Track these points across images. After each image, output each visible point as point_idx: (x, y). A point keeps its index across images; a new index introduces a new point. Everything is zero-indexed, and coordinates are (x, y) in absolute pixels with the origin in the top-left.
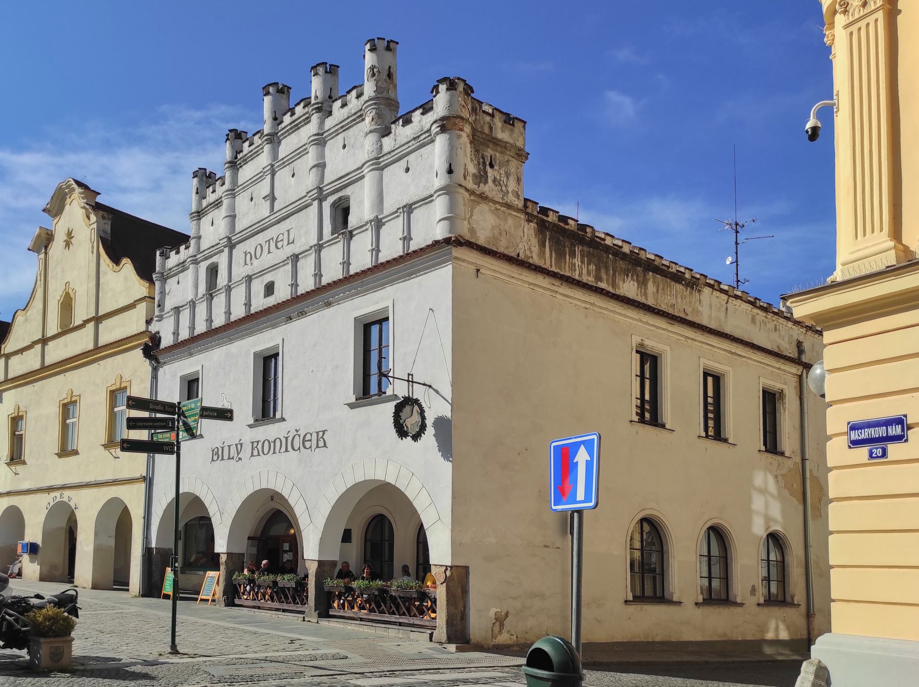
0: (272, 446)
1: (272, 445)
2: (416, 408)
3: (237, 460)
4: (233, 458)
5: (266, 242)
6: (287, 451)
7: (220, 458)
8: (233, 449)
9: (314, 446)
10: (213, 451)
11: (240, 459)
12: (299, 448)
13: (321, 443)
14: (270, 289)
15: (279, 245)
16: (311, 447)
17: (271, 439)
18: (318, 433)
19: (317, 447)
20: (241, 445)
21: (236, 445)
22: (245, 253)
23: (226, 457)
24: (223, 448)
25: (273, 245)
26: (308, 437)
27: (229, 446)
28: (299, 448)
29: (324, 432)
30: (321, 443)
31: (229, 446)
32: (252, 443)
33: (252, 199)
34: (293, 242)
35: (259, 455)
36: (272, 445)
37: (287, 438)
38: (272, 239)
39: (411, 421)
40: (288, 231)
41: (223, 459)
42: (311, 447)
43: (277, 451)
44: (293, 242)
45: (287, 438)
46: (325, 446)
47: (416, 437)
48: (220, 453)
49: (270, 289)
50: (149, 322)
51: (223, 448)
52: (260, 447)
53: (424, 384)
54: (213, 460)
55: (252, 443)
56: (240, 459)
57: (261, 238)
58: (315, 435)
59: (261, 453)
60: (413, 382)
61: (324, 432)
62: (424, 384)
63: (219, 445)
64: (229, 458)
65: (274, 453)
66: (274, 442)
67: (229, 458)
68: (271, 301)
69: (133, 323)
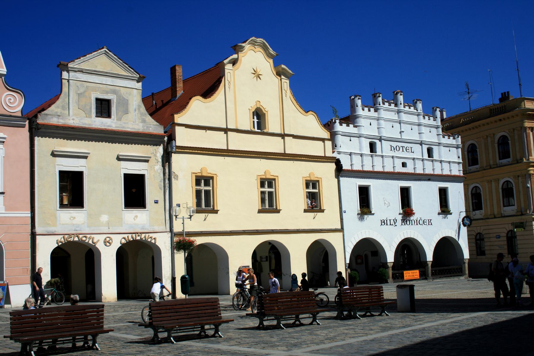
3: (395, 226)
4: (392, 225)
5: (401, 147)
6: (417, 224)
8: (392, 221)
9: (428, 224)
10: (381, 221)
11: (396, 225)
12: (422, 224)
13: (430, 224)
16: (426, 224)
18: (428, 220)
19: (429, 224)
20: (396, 220)
21: (394, 220)
22: (391, 146)
24: (387, 220)
26: (425, 221)
28: (422, 224)
30: (430, 224)
31: (390, 220)
34: (413, 152)
35: (405, 225)
37: (417, 220)
38: (404, 147)
42: (426, 224)
43: (413, 224)
45: (417, 220)
46: (431, 224)
48: (385, 222)
51: (387, 220)
54: (382, 225)
56: (396, 225)
58: (427, 221)
61: (431, 220)
63: (385, 219)
64: (390, 225)
65: (412, 225)
67: (390, 225)
68: (404, 170)
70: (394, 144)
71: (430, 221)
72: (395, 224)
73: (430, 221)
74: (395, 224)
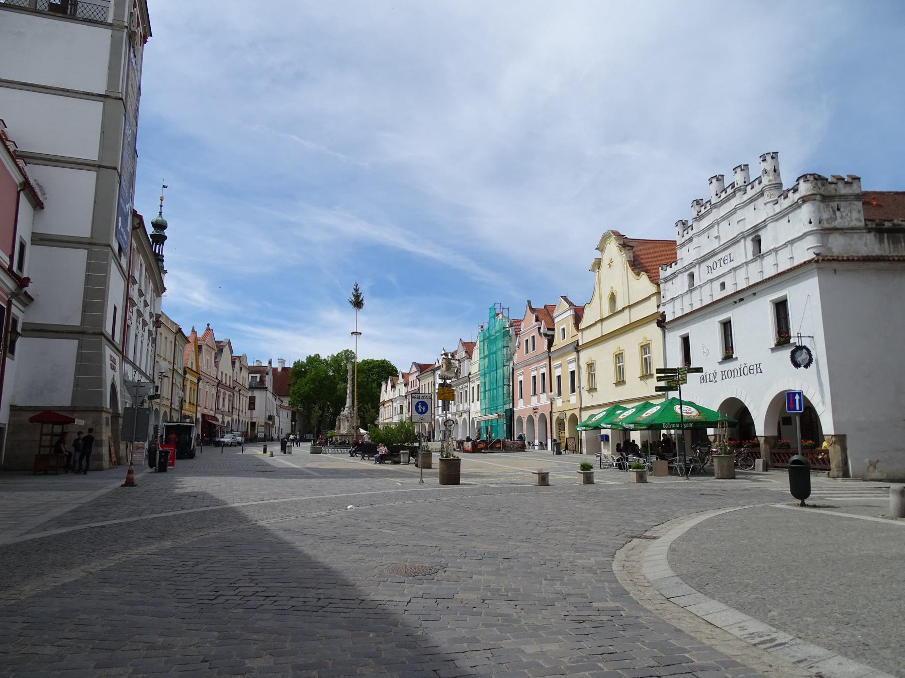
0: (732, 373)
1: (733, 372)
2: (804, 350)
7: (705, 381)
8: (712, 375)
9: (755, 372)
11: (716, 381)
13: (759, 371)
14: (723, 285)
15: (726, 262)
17: (732, 370)
18: (756, 365)
19: (757, 373)
20: (716, 373)
21: (713, 373)
23: (708, 380)
24: (706, 375)
25: (722, 262)
26: (751, 368)
27: (709, 374)
29: (760, 364)
30: (759, 371)
31: (709, 374)
32: (722, 372)
33: (708, 237)
34: (733, 260)
35: (726, 378)
36: (733, 372)
37: (740, 369)
39: (802, 357)
40: (730, 254)
41: (706, 382)
43: (736, 376)
44: (733, 260)
45: (740, 369)
46: (761, 372)
47: (806, 366)
48: (705, 378)
49: (723, 285)
50: (658, 306)
51: (706, 375)
52: (726, 372)
53: (809, 337)
55: (722, 372)
57: (716, 259)
58: (755, 366)
59: (727, 378)
60: (801, 337)
61: (760, 364)
62: (809, 337)
65: (734, 377)
66: (734, 371)
69: (649, 309)
70: (710, 263)
71: (758, 365)
72: (715, 379)
73: (758, 365)
74: (715, 379)
